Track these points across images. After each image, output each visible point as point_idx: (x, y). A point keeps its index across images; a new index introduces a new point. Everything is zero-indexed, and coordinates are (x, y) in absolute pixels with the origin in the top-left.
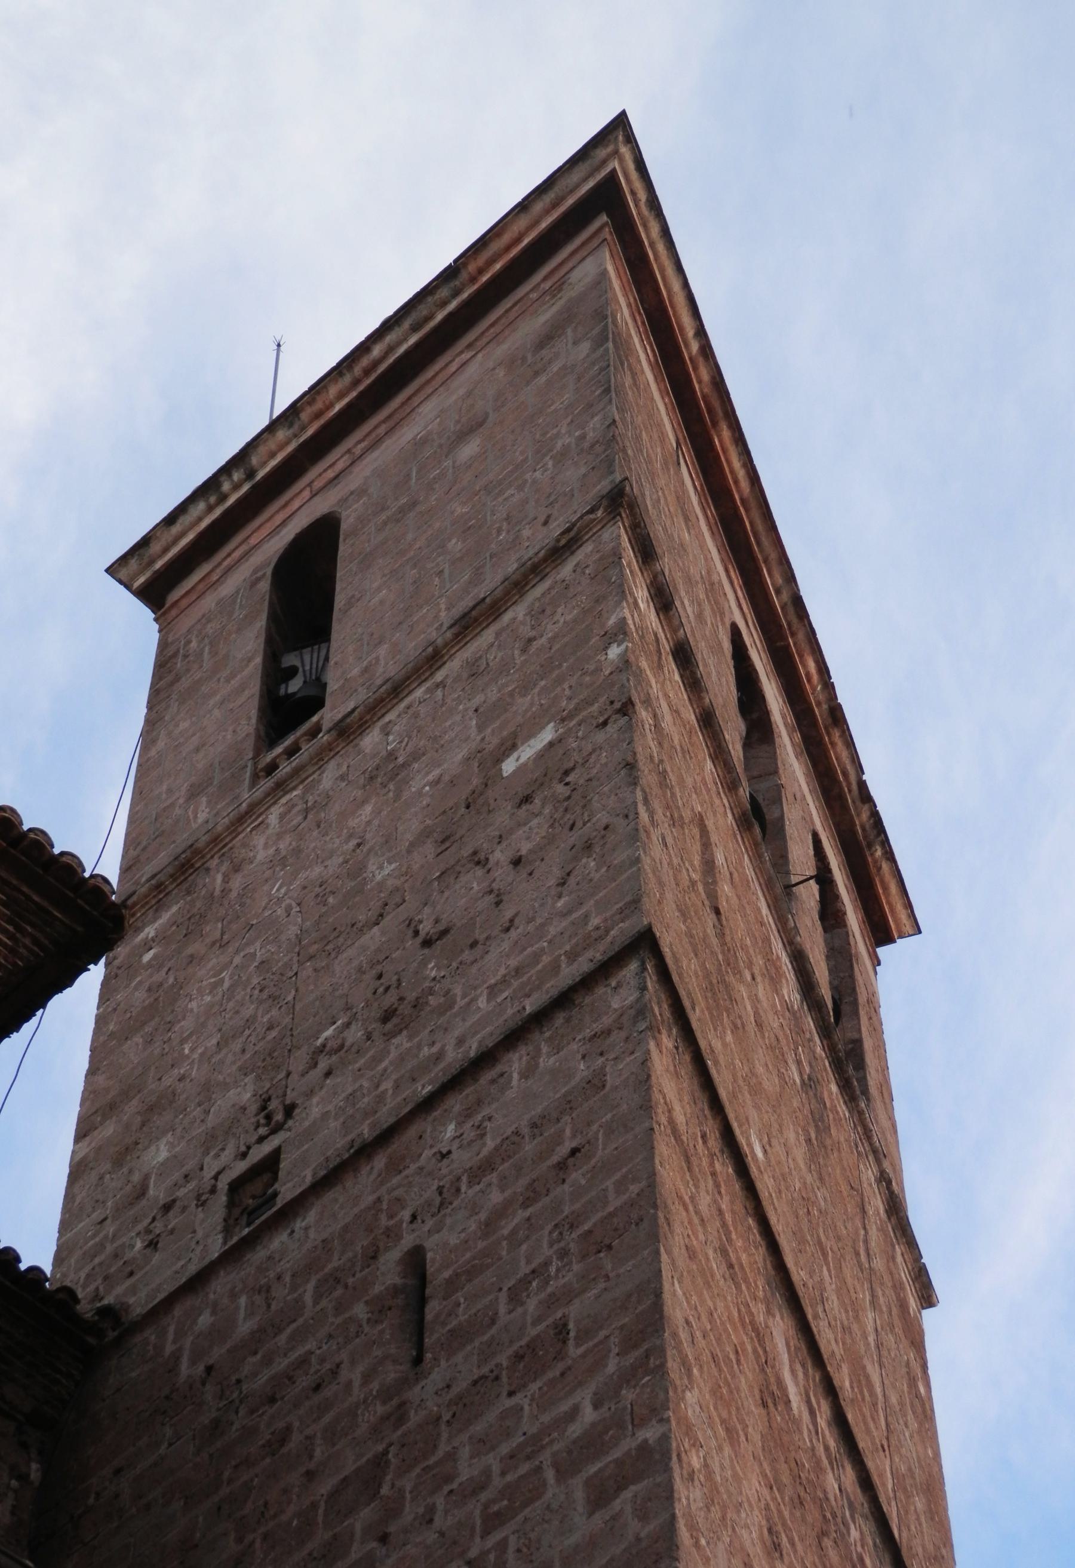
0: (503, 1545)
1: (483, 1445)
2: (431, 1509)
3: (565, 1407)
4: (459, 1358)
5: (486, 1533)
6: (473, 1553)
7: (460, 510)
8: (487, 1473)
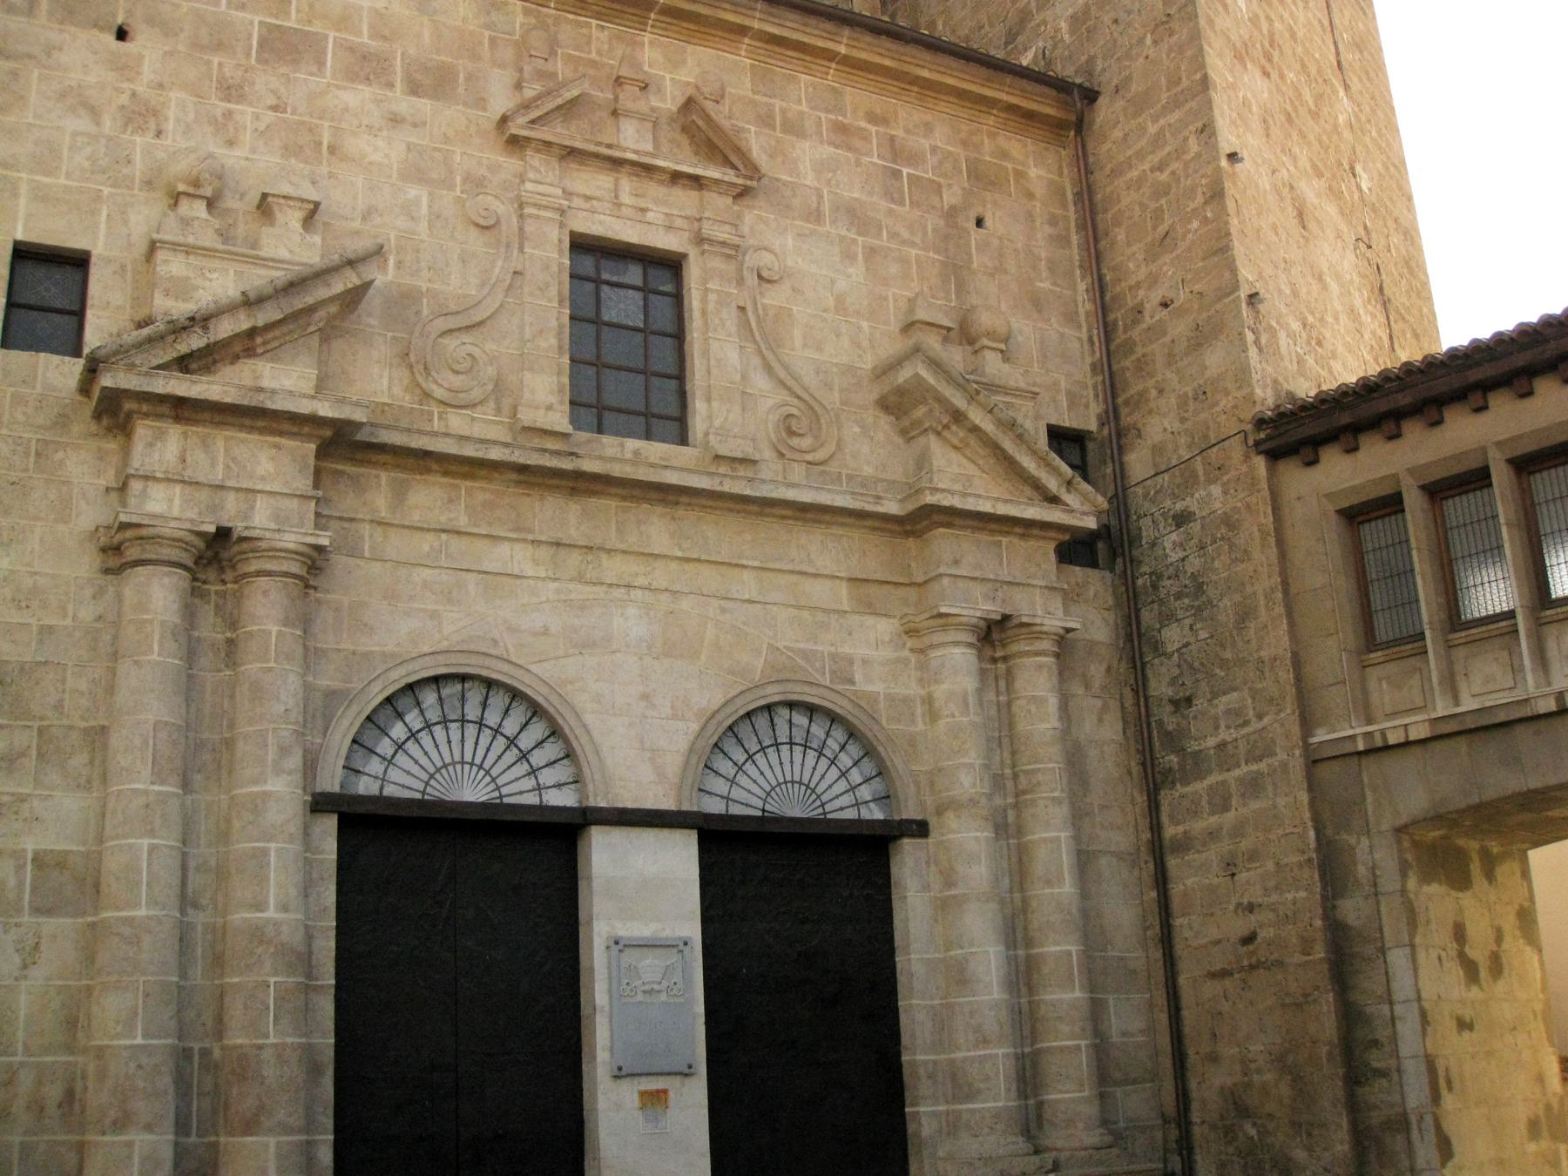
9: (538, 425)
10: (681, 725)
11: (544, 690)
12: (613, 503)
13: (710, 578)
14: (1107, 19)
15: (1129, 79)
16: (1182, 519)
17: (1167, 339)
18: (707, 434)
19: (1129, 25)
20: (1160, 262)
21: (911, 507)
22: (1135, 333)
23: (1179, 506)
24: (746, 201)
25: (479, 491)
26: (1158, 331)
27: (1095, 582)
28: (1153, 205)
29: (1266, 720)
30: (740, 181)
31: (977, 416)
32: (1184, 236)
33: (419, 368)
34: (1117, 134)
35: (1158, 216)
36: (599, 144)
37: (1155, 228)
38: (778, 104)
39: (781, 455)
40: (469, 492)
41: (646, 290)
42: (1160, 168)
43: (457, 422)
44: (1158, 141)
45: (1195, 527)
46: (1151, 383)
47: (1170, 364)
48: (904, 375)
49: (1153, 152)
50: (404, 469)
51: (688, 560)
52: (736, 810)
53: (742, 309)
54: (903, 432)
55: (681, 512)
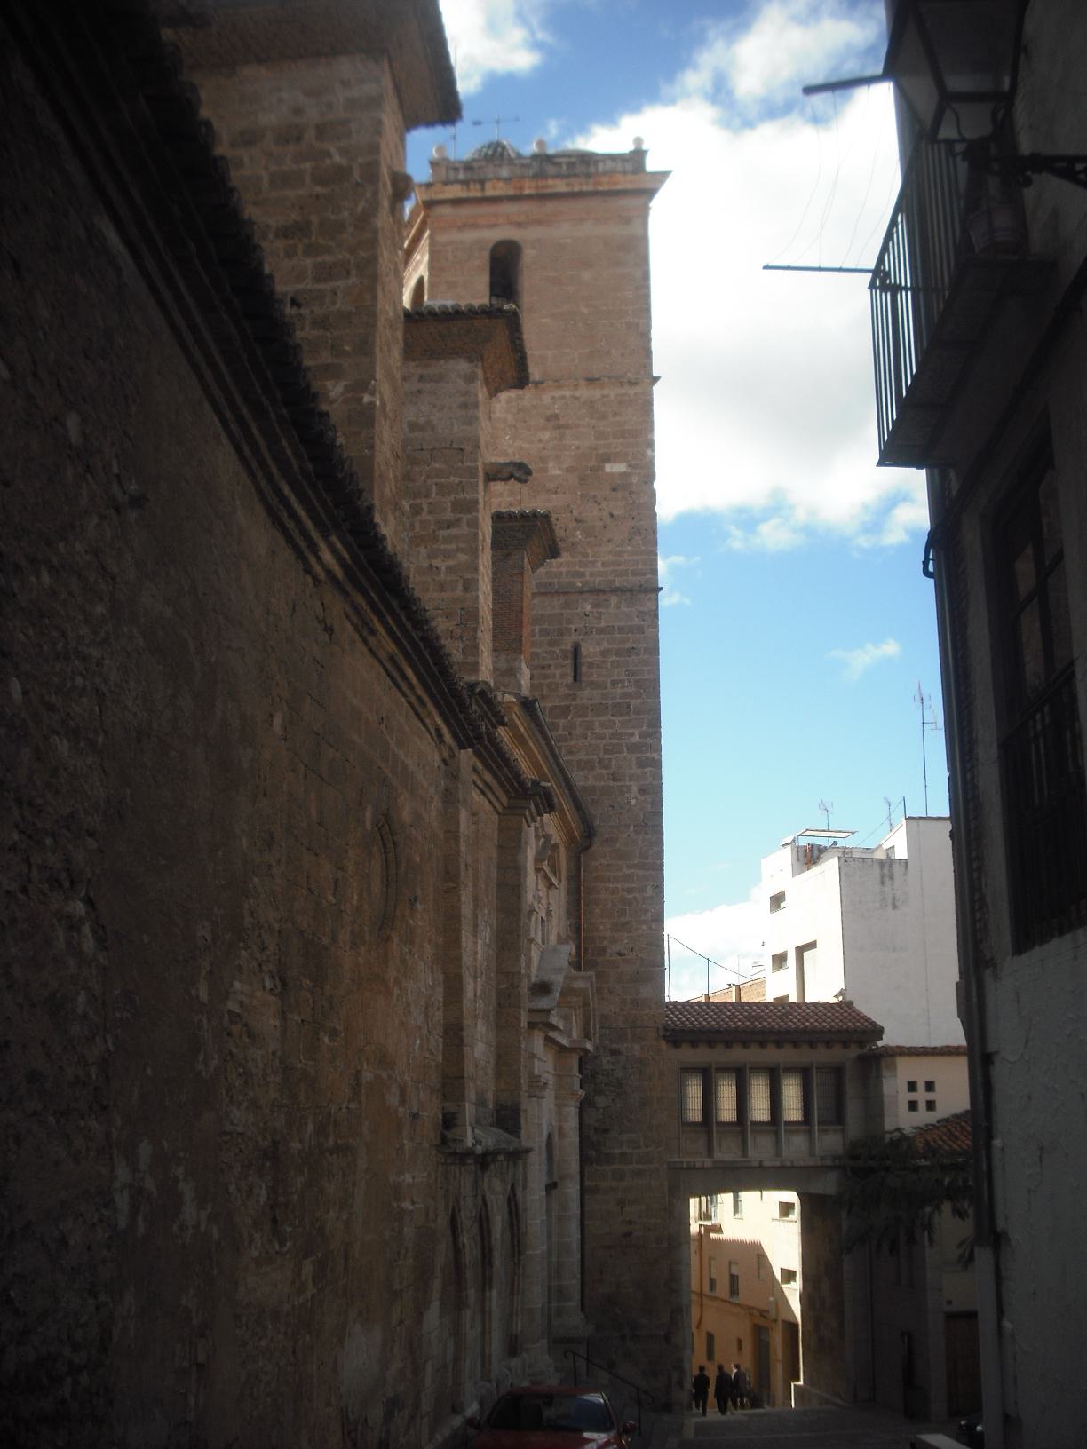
1: (603, 725)
3: (630, 731)
7: (585, 311)
16: (614, 1052)
22: (599, 959)
23: (614, 1046)
29: (650, 1149)
32: (636, 930)
34: (603, 861)
42: (629, 891)
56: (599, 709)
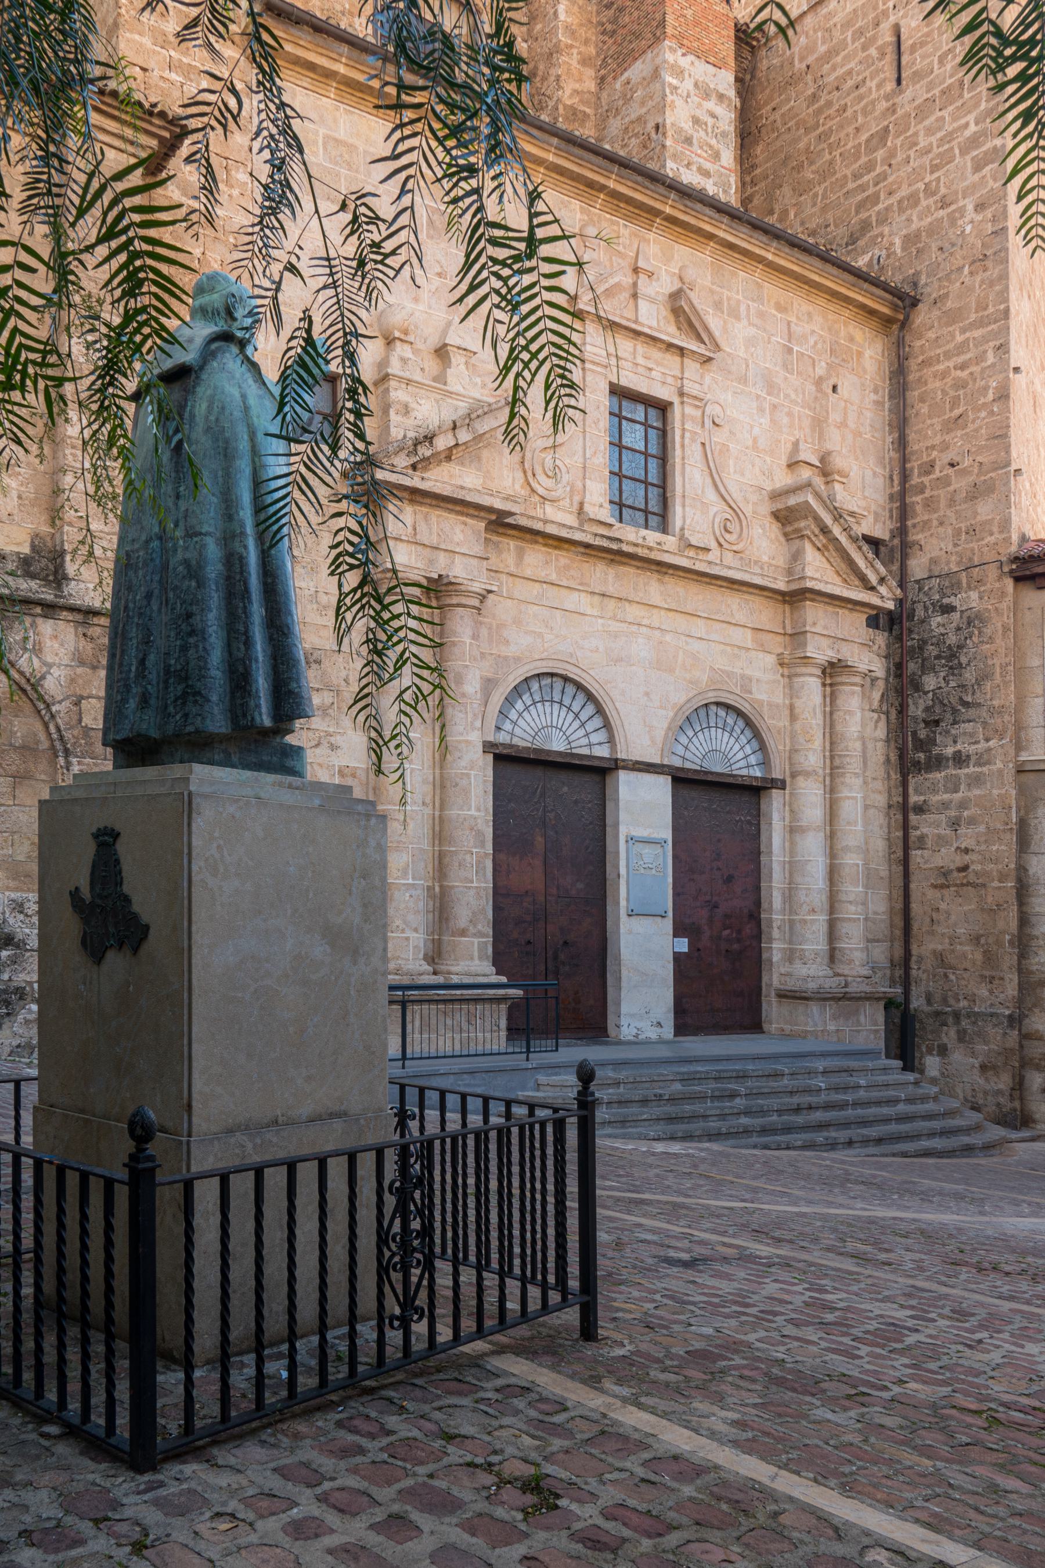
0: (938, 179)
1: (930, 131)
2: (909, 157)
4: (918, 86)
5: (932, 172)
6: (927, 180)
8: (931, 144)
9: (598, 518)
10: (664, 712)
11: (597, 686)
12: (632, 570)
13: (681, 623)
14: (934, 247)
15: (946, 295)
17: (951, 488)
18: (682, 529)
19: (951, 254)
20: (953, 434)
21: (794, 586)
24: (707, 366)
25: (563, 558)
26: (945, 481)
27: (881, 639)
28: (952, 393)
30: (707, 354)
31: (837, 531)
33: (529, 474)
35: (955, 403)
36: (622, 317)
37: (951, 410)
38: (726, 293)
39: (721, 545)
40: (557, 560)
41: (646, 425)
42: (962, 367)
43: (550, 512)
44: (961, 349)
45: (956, 616)
46: (936, 515)
47: (950, 506)
48: (792, 501)
49: (958, 355)
50: (523, 539)
51: (670, 610)
52: (688, 765)
53: (703, 444)
54: (785, 535)
55: (667, 578)
56: (922, 112)
